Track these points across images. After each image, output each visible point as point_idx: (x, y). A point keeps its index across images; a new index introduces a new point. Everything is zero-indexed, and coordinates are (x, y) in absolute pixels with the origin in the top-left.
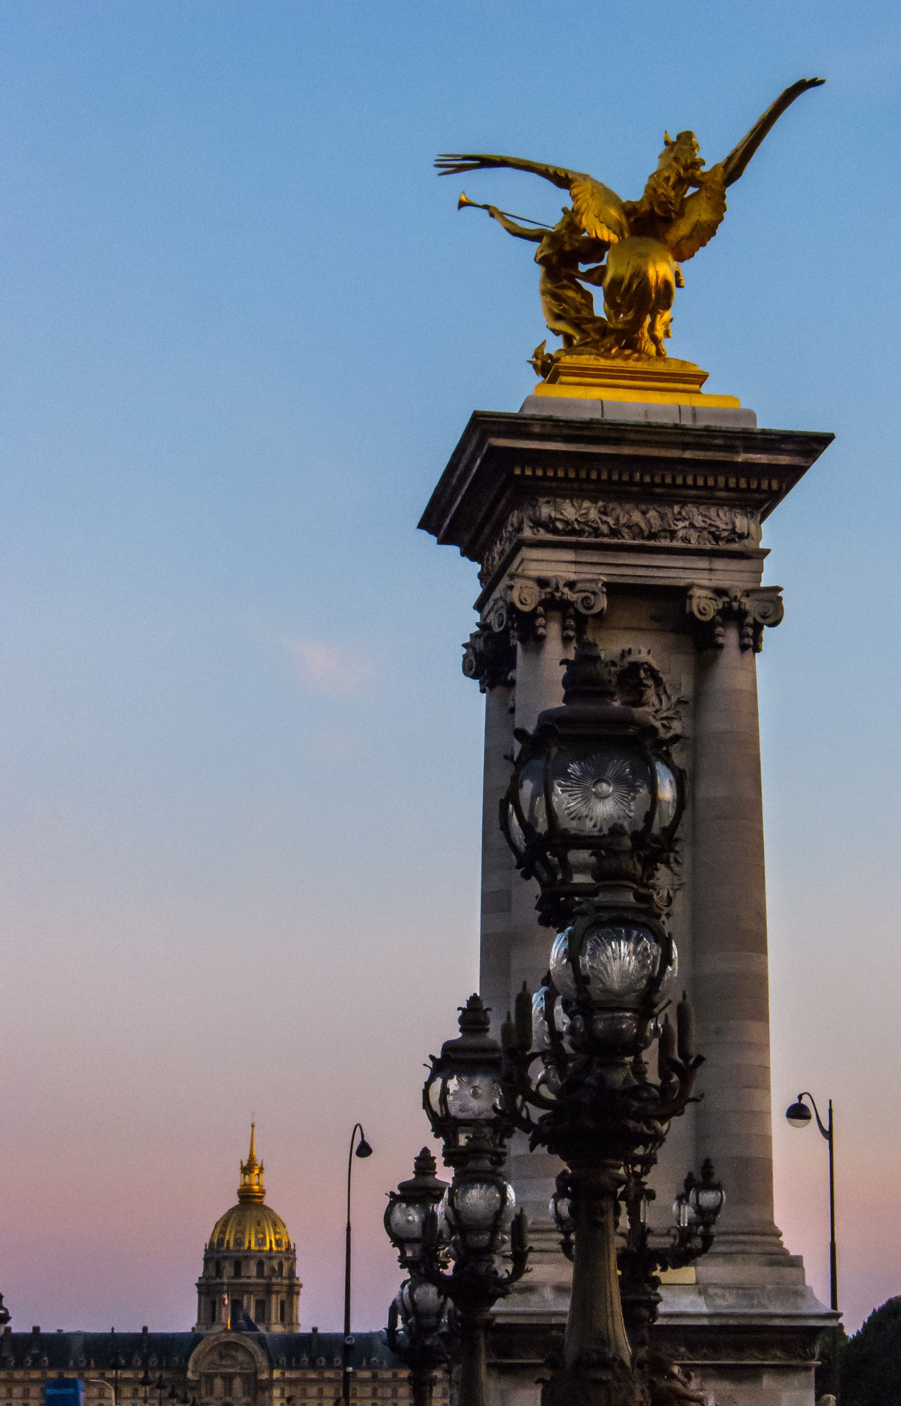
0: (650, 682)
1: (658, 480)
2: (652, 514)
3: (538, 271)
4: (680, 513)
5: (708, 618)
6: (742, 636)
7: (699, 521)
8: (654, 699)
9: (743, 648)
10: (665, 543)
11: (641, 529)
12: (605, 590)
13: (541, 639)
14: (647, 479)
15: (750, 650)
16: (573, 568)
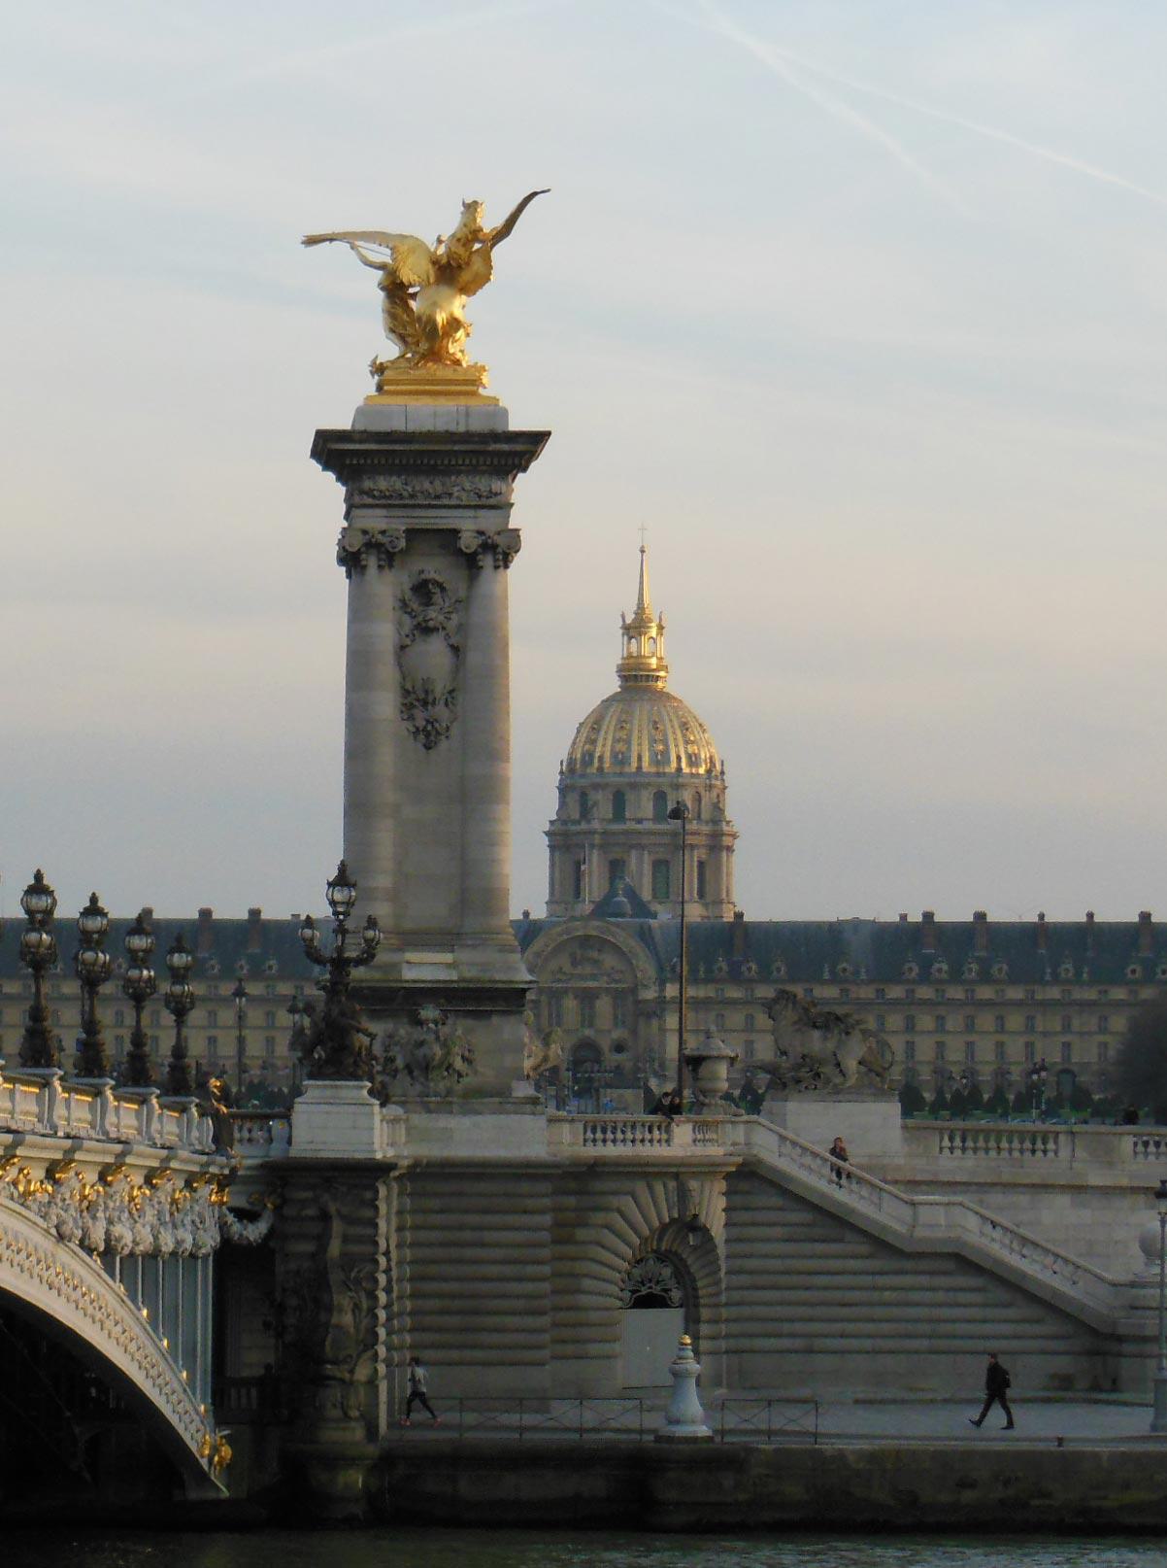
0: (438, 590)
1: (439, 462)
2: (437, 483)
3: (381, 295)
4: (455, 481)
5: (473, 550)
6: (496, 560)
7: (467, 486)
8: (440, 601)
9: (497, 567)
10: (446, 501)
11: (429, 493)
12: (404, 535)
13: (364, 567)
14: (432, 462)
15: (502, 568)
16: (386, 520)
